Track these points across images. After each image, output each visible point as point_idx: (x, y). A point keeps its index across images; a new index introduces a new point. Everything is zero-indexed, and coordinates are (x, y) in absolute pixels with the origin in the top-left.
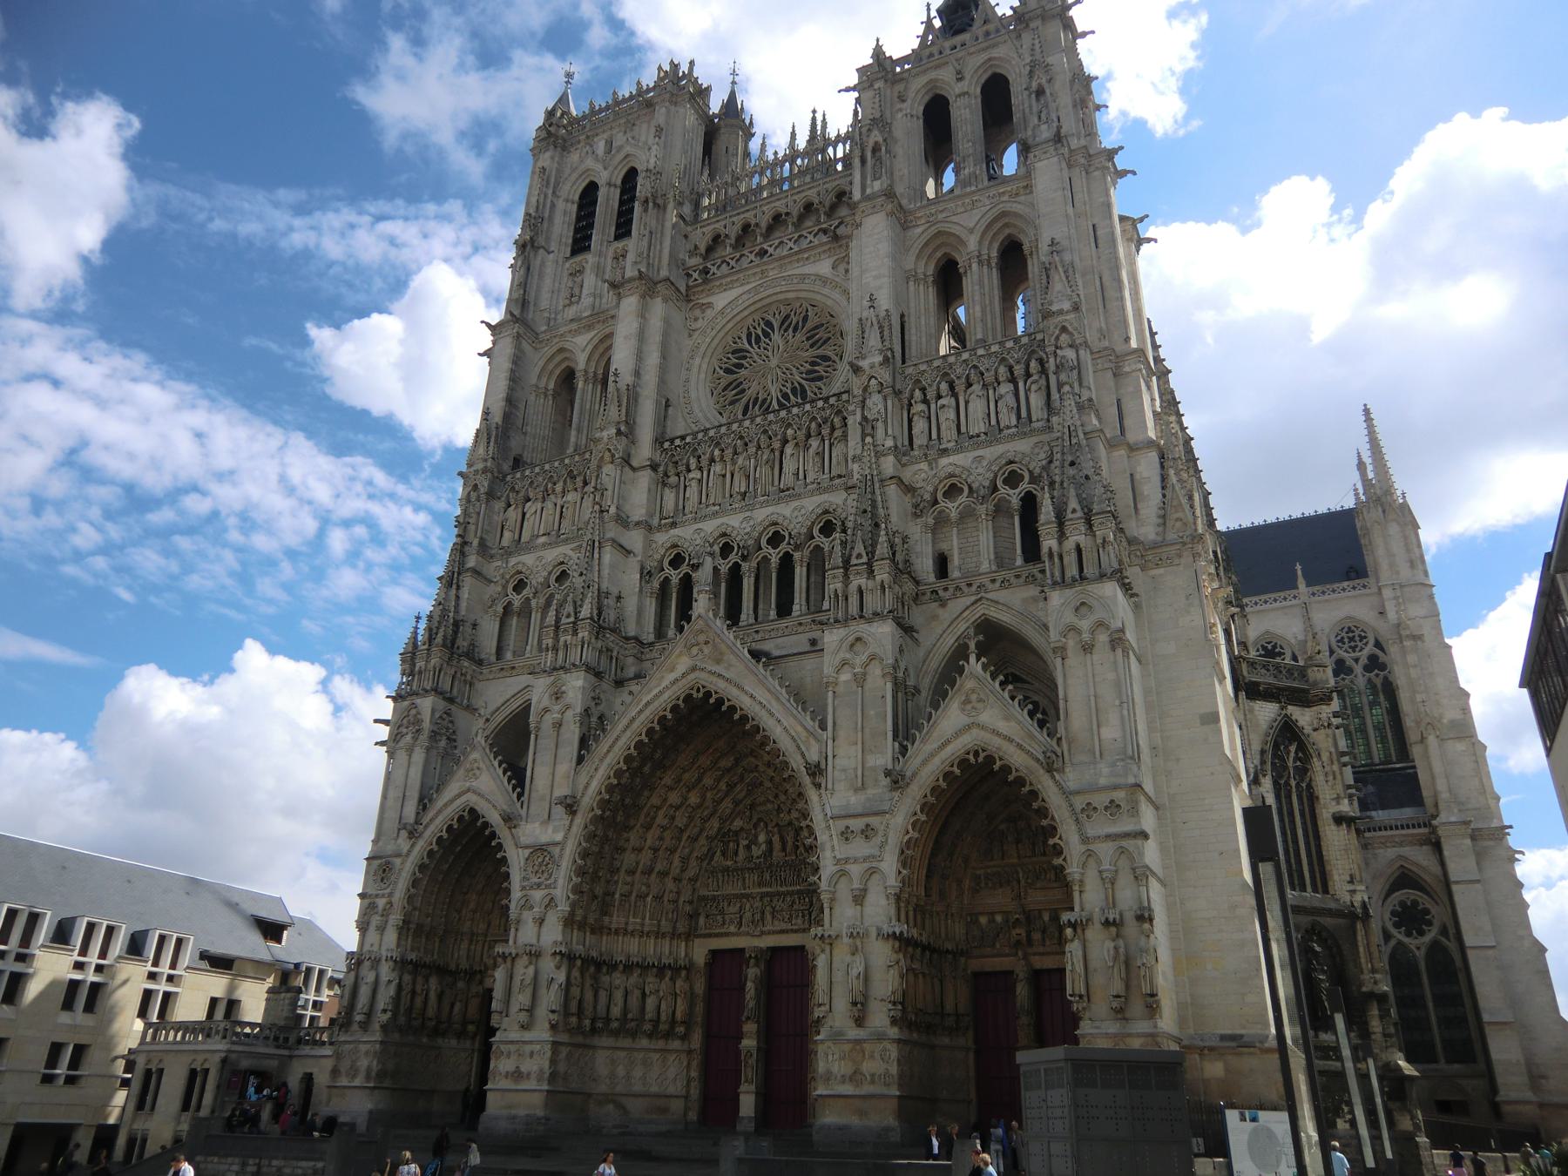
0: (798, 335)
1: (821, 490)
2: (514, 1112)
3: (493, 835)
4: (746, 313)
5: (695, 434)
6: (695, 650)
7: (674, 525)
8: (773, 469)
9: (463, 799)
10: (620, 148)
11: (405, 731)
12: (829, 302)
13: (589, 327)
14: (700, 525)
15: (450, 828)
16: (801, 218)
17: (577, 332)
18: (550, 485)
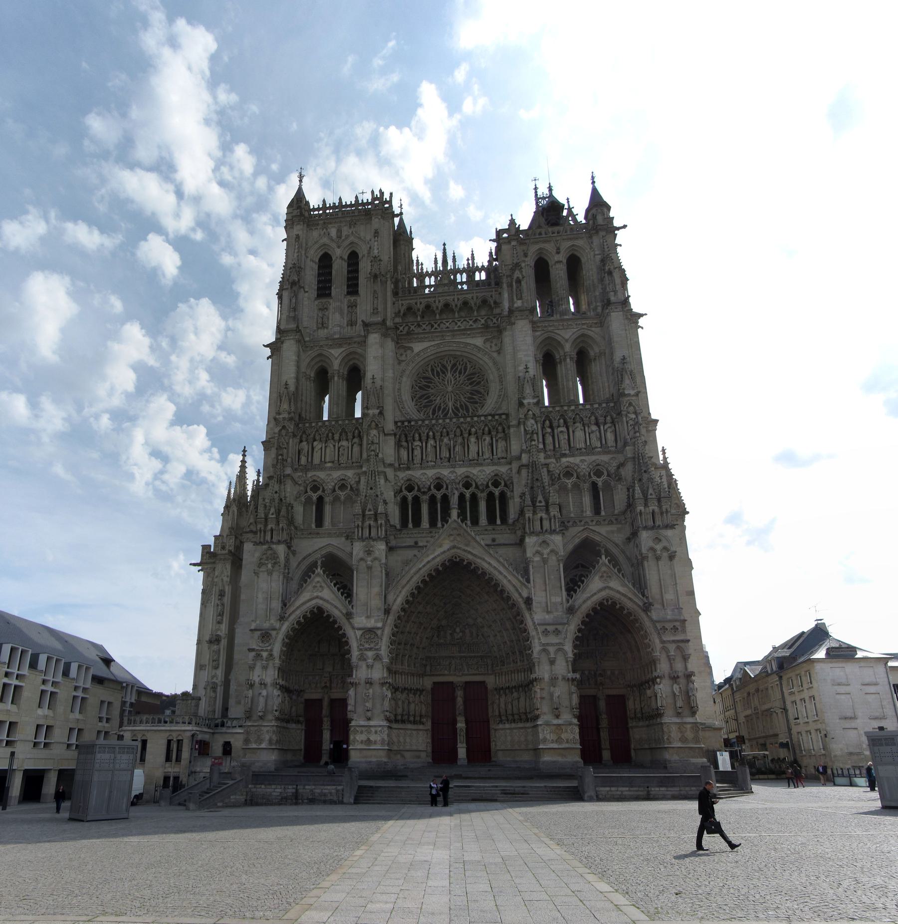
0: (462, 377)
1: (494, 464)
2: (369, 759)
3: (335, 622)
4: (432, 357)
5: (416, 421)
6: (452, 538)
7: (408, 468)
8: (464, 447)
9: (314, 602)
10: (347, 237)
11: (266, 562)
12: (481, 362)
13: (340, 346)
14: (424, 471)
15: (305, 617)
16: (461, 309)
17: (331, 347)
18: (330, 434)
